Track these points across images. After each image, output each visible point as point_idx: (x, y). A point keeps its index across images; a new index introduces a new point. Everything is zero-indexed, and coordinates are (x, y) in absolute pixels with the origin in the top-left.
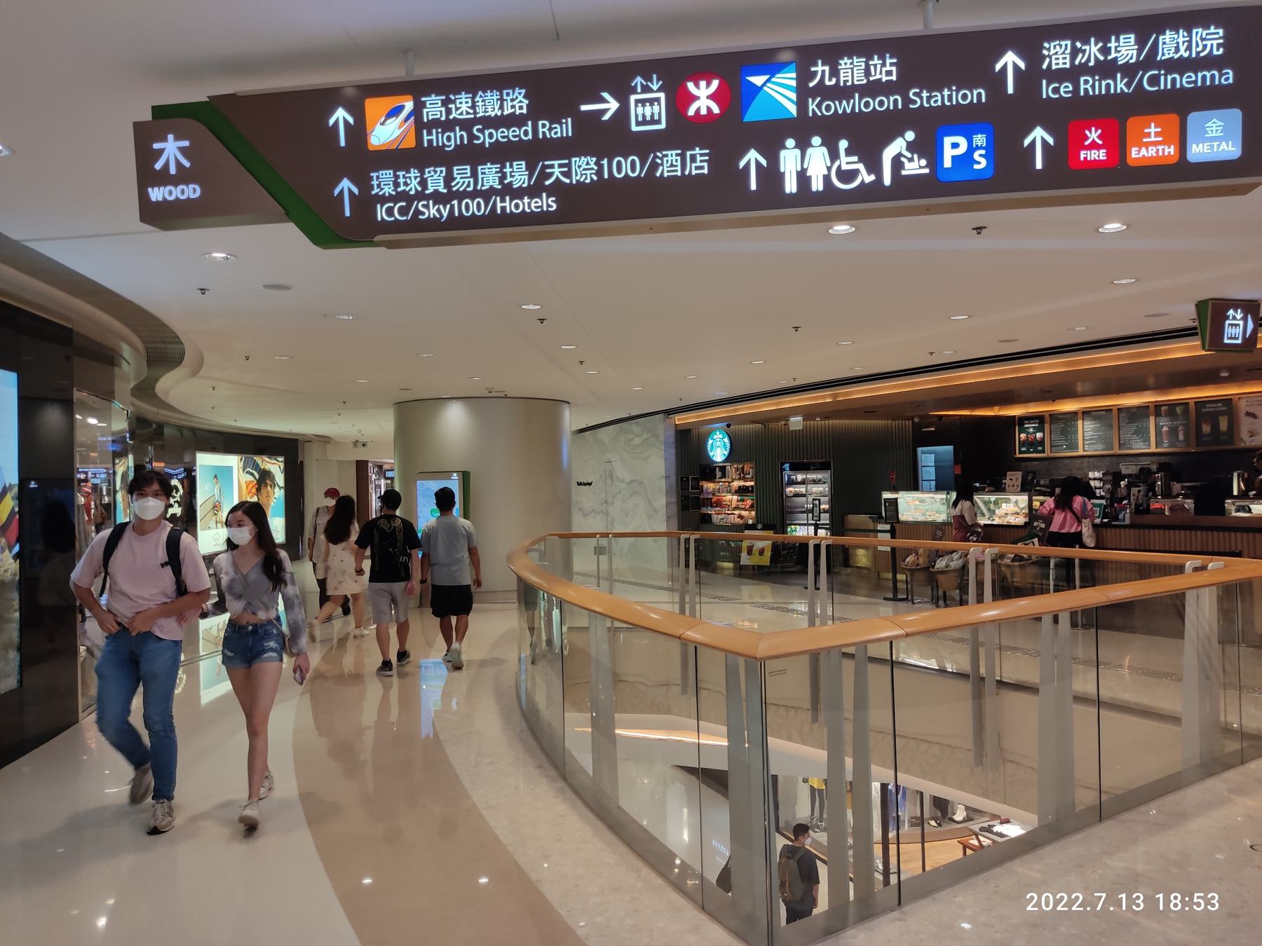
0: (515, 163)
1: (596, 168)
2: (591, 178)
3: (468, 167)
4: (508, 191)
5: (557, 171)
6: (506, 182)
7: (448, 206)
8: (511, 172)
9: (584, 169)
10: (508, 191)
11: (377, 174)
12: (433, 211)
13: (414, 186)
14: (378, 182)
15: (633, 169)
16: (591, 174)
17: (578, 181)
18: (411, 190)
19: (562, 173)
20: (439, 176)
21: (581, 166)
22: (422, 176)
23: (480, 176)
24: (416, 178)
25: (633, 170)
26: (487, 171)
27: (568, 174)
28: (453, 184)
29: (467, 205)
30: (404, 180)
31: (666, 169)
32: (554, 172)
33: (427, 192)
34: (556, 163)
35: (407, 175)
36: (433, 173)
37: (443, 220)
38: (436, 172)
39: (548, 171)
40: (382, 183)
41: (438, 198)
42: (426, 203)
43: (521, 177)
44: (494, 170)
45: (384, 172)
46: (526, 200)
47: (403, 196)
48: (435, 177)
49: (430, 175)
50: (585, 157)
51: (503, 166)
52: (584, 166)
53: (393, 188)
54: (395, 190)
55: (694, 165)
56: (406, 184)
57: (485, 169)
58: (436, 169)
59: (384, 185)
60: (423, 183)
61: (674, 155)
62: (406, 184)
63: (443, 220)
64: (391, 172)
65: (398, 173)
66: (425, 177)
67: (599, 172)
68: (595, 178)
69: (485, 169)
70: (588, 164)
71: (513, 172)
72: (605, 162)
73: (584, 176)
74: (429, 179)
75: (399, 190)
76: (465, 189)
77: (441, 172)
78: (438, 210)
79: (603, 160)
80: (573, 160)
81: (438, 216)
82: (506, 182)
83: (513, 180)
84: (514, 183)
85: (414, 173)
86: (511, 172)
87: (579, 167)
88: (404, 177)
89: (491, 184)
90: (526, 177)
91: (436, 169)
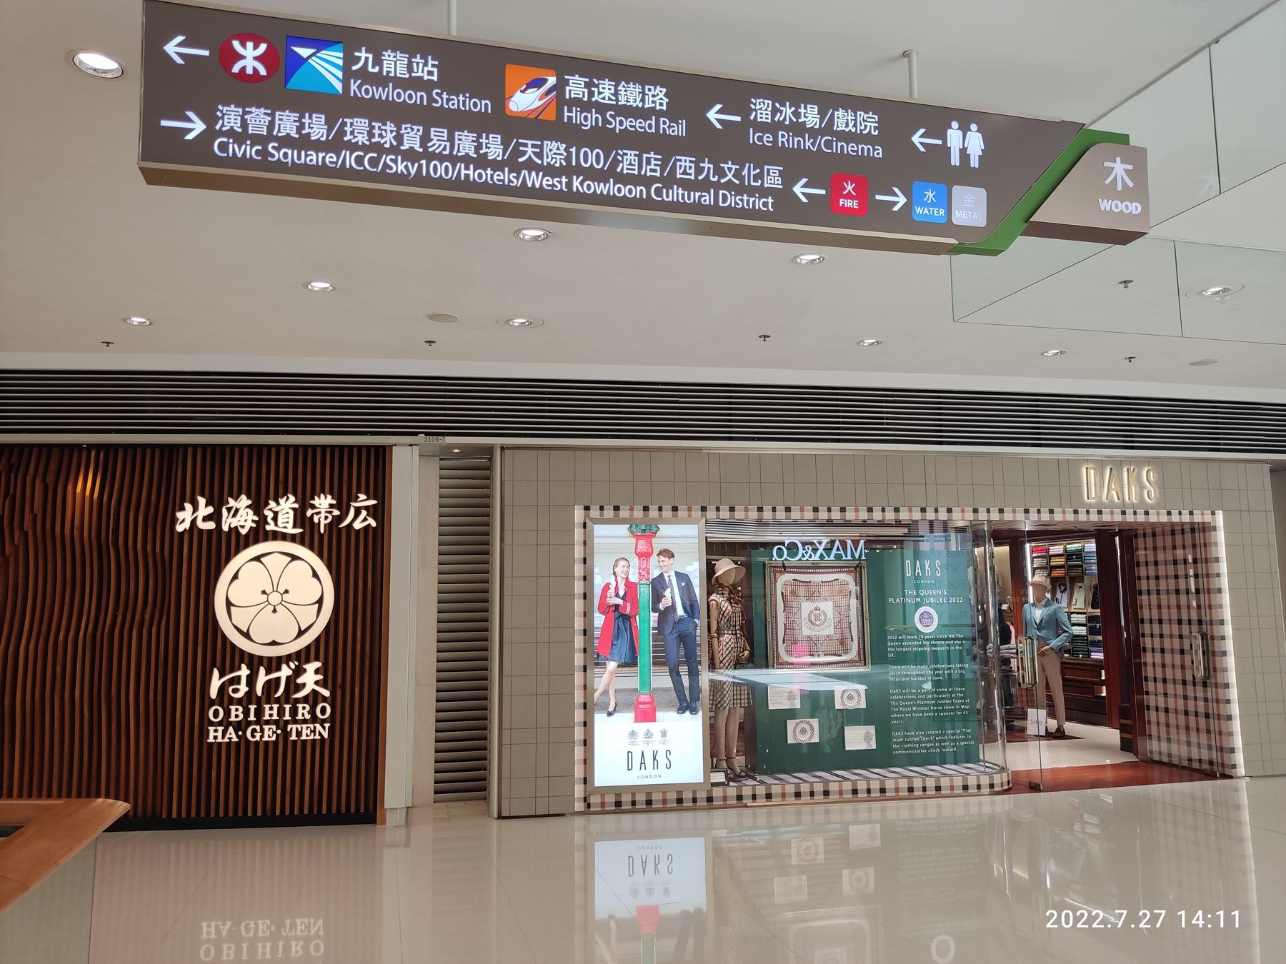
2: (561, 163)
3: (446, 131)
4: (481, 161)
5: (530, 150)
7: (416, 165)
10: (481, 161)
11: (352, 121)
12: (401, 167)
13: (389, 140)
14: (352, 129)
16: (560, 159)
17: (548, 163)
18: (386, 142)
20: (416, 134)
23: (457, 142)
24: (392, 131)
26: (463, 138)
27: (540, 155)
28: (429, 145)
29: (435, 166)
30: (380, 132)
31: (625, 167)
32: (526, 151)
33: (402, 148)
34: (530, 142)
35: (382, 127)
36: (409, 130)
37: (410, 178)
38: (412, 130)
40: (356, 131)
41: (411, 156)
42: (394, 157)
43: (496, 150)
44: (471, 139)
45: (359, 120)
46: (489, 172)
48: (412, 134)
49: (406, 131)
52: (555, 151)
54: (369, 140)
55: (649, 167)
56: (380, 136)
57: (461, 135)
58: (413, 127)
59: (358, 133)
60: (399, 138)
61: (633, 155)
62: (380, 136)
63: (410, 178)
64: (367, 121)
65: (373, 124)
66: (402, 132)
67: (568, 159)
69: (461, 135)
73: (554, 160)
74: (405, 135)
75: (373, 140)
76: (441, 152)
77: (418, 130)
78: (406, 167)
79: (572, 148)
82: (481, 152)
86: (486, 144)
87: (551, 150)
89: (467, 151)
91: (413, 127)
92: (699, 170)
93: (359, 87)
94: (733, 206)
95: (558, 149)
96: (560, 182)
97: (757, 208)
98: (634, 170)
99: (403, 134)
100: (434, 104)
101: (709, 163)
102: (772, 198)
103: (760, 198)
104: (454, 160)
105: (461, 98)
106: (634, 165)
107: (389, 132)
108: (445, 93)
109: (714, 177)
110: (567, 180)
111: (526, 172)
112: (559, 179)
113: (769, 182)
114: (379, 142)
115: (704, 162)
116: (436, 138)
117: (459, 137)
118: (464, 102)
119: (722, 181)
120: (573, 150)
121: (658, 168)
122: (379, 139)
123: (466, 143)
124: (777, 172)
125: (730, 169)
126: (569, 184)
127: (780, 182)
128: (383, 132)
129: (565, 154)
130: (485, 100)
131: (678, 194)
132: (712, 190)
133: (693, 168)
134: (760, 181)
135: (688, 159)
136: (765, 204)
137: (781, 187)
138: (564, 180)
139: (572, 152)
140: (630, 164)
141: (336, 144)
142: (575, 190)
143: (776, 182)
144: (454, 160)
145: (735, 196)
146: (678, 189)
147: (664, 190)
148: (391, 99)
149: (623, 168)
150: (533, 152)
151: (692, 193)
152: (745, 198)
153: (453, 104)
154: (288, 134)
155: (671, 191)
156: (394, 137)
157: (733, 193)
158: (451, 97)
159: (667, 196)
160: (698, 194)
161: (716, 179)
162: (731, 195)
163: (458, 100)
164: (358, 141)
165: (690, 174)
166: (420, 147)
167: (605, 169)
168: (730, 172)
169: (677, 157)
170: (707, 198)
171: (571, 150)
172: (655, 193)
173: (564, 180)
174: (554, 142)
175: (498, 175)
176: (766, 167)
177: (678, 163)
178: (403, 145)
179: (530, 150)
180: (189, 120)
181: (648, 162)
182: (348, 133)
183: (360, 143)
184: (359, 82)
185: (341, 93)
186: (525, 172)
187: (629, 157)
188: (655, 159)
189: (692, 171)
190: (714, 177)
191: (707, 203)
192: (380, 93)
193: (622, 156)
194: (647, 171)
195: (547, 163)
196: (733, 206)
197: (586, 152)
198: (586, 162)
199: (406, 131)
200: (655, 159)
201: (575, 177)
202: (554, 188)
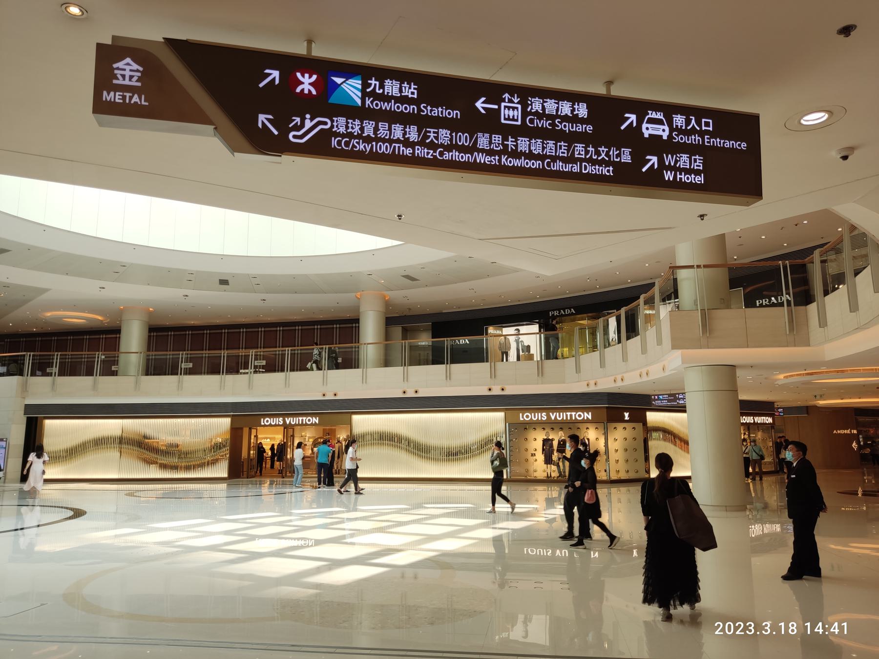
3: (387, 124)
4: (407, 143)
6: (406, 137)
7: (370, 145)
12: (362, 147)
13: (356, 130)
18: (355, 132)
20: (371, 126)
23: (393, 131)
28: (378, 133)
33: (364, 135)
35: (354, 123)
36: (368, 124)
40: (339, 125)
41: (368, 140)
44: (401, 129)
45: (341, 118)
47: (351, 136)
48: (369, 127)
51: (405, 127)
54: (346, 131)
56: (352, 128)
58: (370, 122)
59: (341, 126)
62: (352, 128)
64: (345, 119)
65: (349, 120)
74: (366, 127)
76: (384, 137)
77: (372, 124)
78: (365, 146)
86: (409, 131)
88: (352, 123)
89: (398, 136)
92: (587, 152)
93: (372, 102)
94: (590, 172)
95: (446, 134)
96: (495, 159)
97: (405, 154)
98: (687, 165)
100: (422, 113)
102: (612, 167)
103: (605, 167)
104: (391, 141)
105: (440, 109)
106: (553, 150)
107: (356, 125)
108: (429, 106)
109: (595, 156)
112: (594, 167)
113: (624, 158)
115: (589, 147)
117: (395, 128)
118: (442, 112)
119: (599, 158)
120: (454, 134)
123: (398, 131)
124: (628, 152)
125: (603, 151)
126: (500, 161)
127: (630, 159)
128: (354, 126)
129: (450, 137)
130: (456, 110)
131: (559, 165)
132: (578, 163)
133: (584, 150)
134: (619, 158)
136: (608, 171)
137: (631, 161)
138: (497, 158)
140: (684, 162)
142: (503, 164)
143: (628, 159)
144: (391, 141)
145: (591, 166)
146: (455, 152)
147: (552, 163)
148: (393, 110)
149: (681, 164)
151: (567, 165)
152: (597, 167)
153: (435, 113)
154: (398, 138)
155: (555, 164)
156: (359, 129)
157: (590, 164)
158: (433, 109)
159: (554, 167)
160: (570, 165)
161: (595, 157)
162: (589, 166)
163: (438, 111)
165: (582, 155)
166: (373, 134)
167: (470, 145)
168: (603, 153)
169: (576, 145)
170: (576, 168)
172: (547, 166)
173: (497, 158)
175: (698, 178)
176: (622, 149)
177: (576, 148)
178: (364, 133)
179: (432, 135)
181: (561, 148)
183: (341, 133)
184: (372, 99)
185: (360, 105)
186: (476, 153)
187: (683, 158)
188: (699, 159)
189: (583, 153)
190: (595, 156)
191: (447, 158)
192: (385, 106)
193: (546, 145)
194: (547, 151)
197: (460, 135)
198: (460, 142)
200: (699, 159)
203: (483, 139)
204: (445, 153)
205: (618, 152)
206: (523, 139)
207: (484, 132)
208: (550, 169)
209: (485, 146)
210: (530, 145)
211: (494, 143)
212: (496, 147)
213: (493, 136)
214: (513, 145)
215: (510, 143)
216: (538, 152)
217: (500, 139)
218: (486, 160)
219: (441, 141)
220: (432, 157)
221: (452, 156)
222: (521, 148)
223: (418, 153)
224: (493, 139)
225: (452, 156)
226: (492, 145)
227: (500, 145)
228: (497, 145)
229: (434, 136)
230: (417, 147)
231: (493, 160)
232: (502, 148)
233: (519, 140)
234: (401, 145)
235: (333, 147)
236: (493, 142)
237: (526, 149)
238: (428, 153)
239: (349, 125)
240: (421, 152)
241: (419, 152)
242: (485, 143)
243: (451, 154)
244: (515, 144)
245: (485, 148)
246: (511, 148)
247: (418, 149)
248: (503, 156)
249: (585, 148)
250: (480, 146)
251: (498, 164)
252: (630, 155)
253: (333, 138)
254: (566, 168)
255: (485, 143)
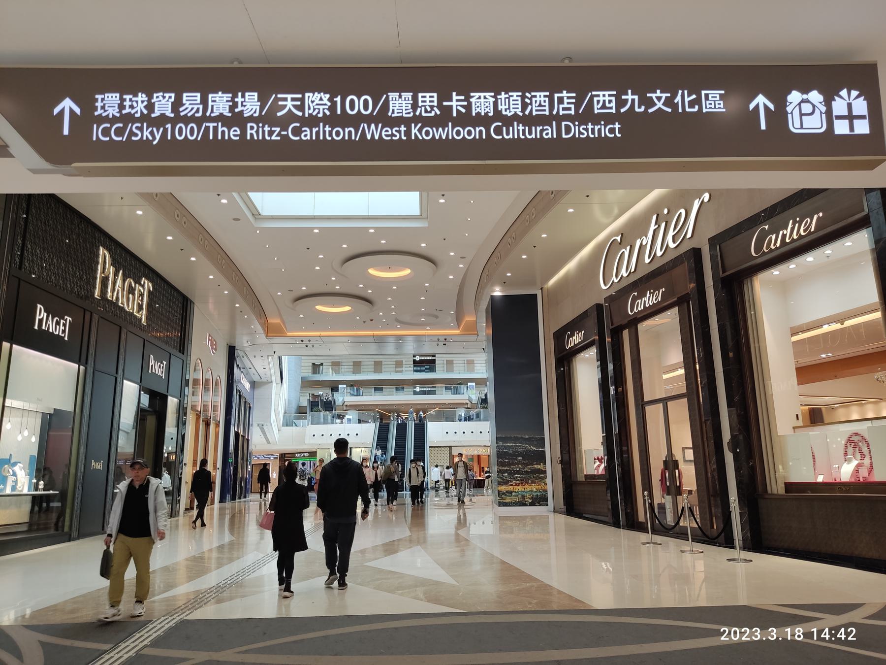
0: (247, 94)
1: (329, 104)
2: (324, 113)
3: (199, 95)
8: (242, 102)
9: (317, 105)
14: (102, 104)
15: (366, 107)
16: (324, 109)
19: (295, 106)
21: (314, 101)
22: (149, 101)
23: (210, 104)
24: (143, 102)
25: (366, 108)
26: (217, 99)
27: (301, 108)
28: (181, 109)
30: (130, 103)
34: (289, 96)
38: (164, 97)
39: (280, 103)
49: (158, 99)
50: (319, 93)
52: (317, 102)
53: (118, 110)
57: (216, 97)
58: (165, 95)
60: (150, 107)
66: (153, 101)
67: (333, 108)
68: (328, 113)
69: (216, 97)
70: (321, 99)
71: (245, 101)
72: (338, 99)
73: (317, 111)
75: (124, 112)
76: (194, 114)
77: (170, 97)
79: (336, 97)
80: (307, 95)
81: (150, 138)
83: (245, 109)
84: (245, 112)
85: (142, 97)
87: (313, 102)
90: (258, 108)
99: (154, 103)
101: (632, 94)
110: (405, 129)
111: (365, 125)
114: (130, 113)
116: (188, 102)
121: (572, 106)
122: (130, 110)
135: (607, 93)
139: (336, 101)
141: (267, 118)
150: (294, 106)
164: (109, 114)
171: (335, 99)
174: (316, 93)
180: (62, 112)
182: (99, 108)
195: (309, 114)
196: (577, 136)
199: (158, 99)
201: (413, 125)
202: (394, 138)
203: (400, 102)
204: (303, 129)
205: (694, 96)
206: (482, 95)
207: (400, 90)
208: (500, 137)
209: (404, 112)
210: (495, 104)
211: (422, 106)
212: (426, 111)
213: (420, 95)
214: (462, 106)
215: (454, 103)
216: (513, 113)
217: (435, 99)
218: (384, 133)
219: (311, 112)
220: (279, 138)
221: (318, 133)
222: (478, 110)
223: (252, 135)
224: (420, 99)
225: (318, 133)
226: (419, 110)
227: (435, 109)
228: (429, 109)
229: (295, 106)
230: (249, 125)
231: (395, 133)
232: (438, 113)
233: (473, 97)
234: (220, 124)
235: (94, 139)
236: (420, 104)
237: (487, 110)
238: (271, 133)
239: (125, 103)
240: (257, 132)
241: (253, 132)
242: (404, 108)
243: (314, 130)
244: (465, 103)
245: (405, 115)
246: (458, 111)
247: (252, 128)
248: (413, 125)
249: (618, 97)
250: (393, 112)
251: (404, 138)
252: (720, 100)
253: (95, 126)
254: (530, 134)
255: (404, 108)
